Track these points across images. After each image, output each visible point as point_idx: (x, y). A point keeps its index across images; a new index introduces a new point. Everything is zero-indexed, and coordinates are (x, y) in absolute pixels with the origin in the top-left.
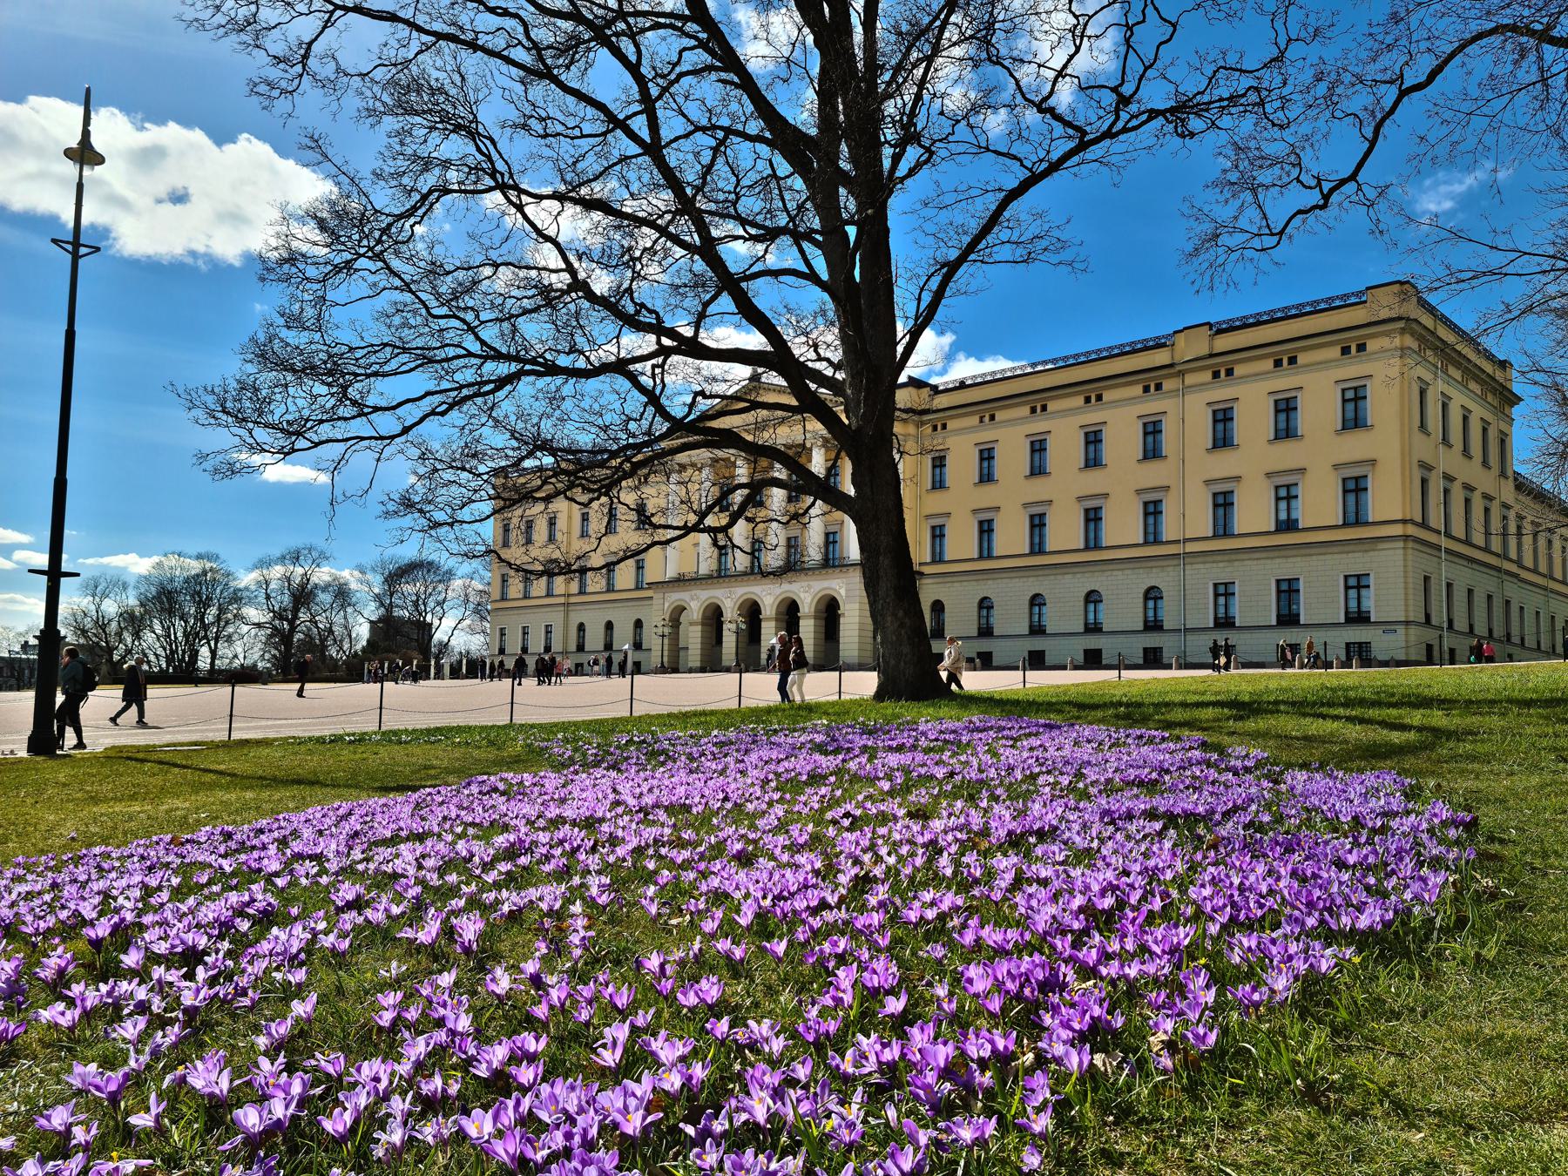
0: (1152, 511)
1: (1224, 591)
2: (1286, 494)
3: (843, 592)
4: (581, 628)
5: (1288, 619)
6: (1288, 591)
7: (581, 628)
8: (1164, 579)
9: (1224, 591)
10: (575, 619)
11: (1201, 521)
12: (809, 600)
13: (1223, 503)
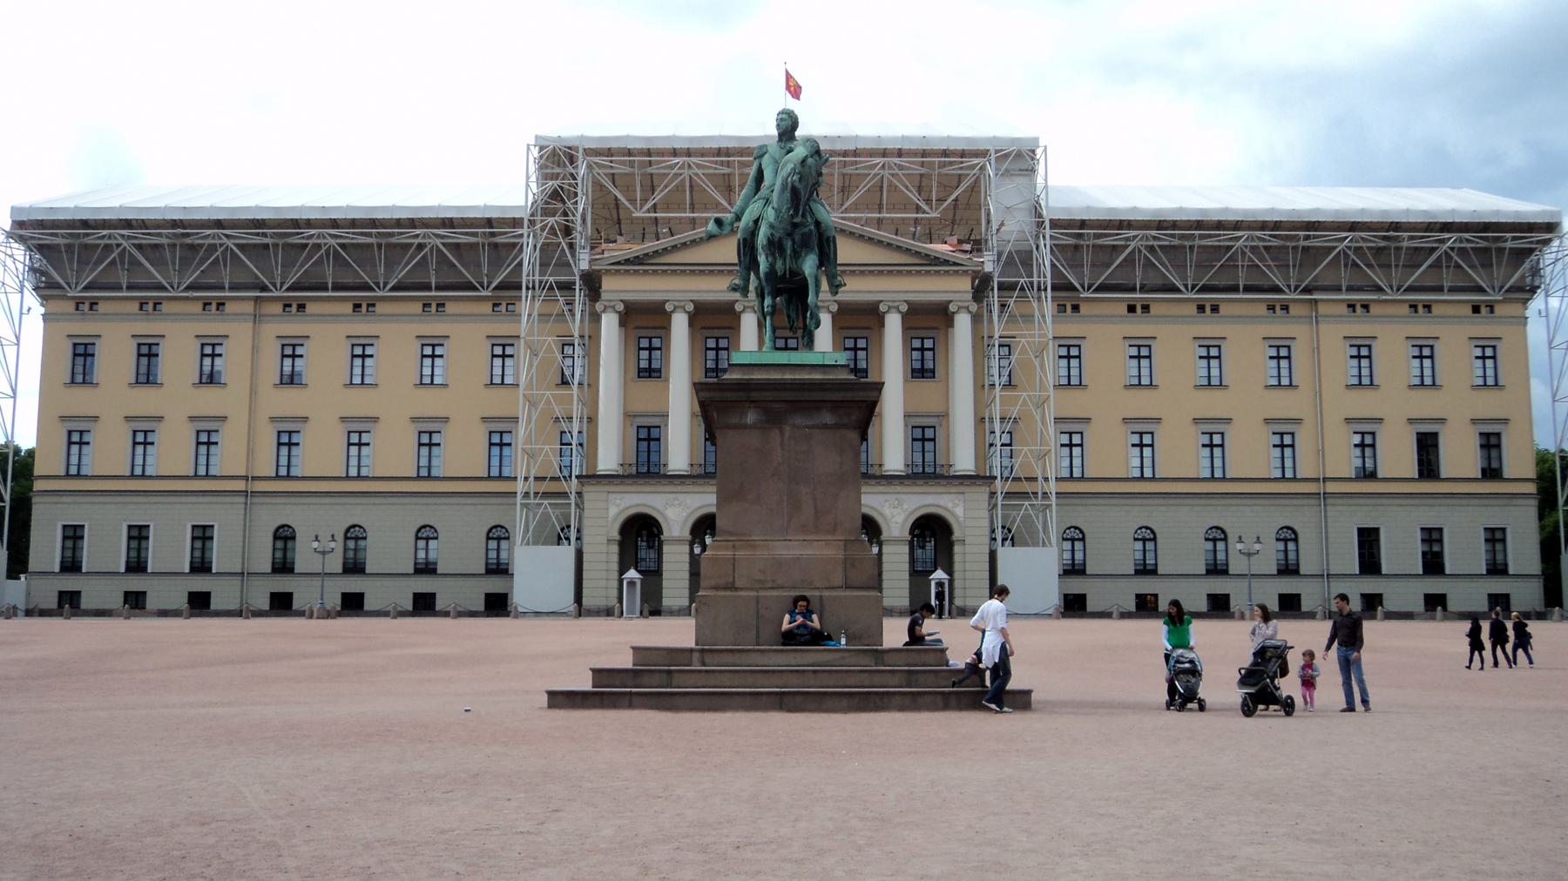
0: (1285, 445)
1: (1368, 540)
2: (1427, 446)
3: (959, 511)
4: (284, 536)
5: (1433, 564)
6: (1432, 537)
7: (284, 536)
8: (1303, 519)
9: (1368, 540)
10: (269, 517)
11: (1343, 460)
12: (900, 518)
13: (1367, 445)
